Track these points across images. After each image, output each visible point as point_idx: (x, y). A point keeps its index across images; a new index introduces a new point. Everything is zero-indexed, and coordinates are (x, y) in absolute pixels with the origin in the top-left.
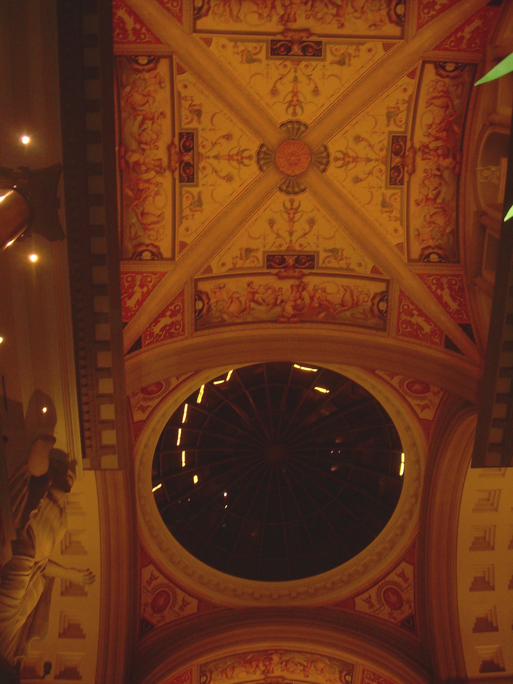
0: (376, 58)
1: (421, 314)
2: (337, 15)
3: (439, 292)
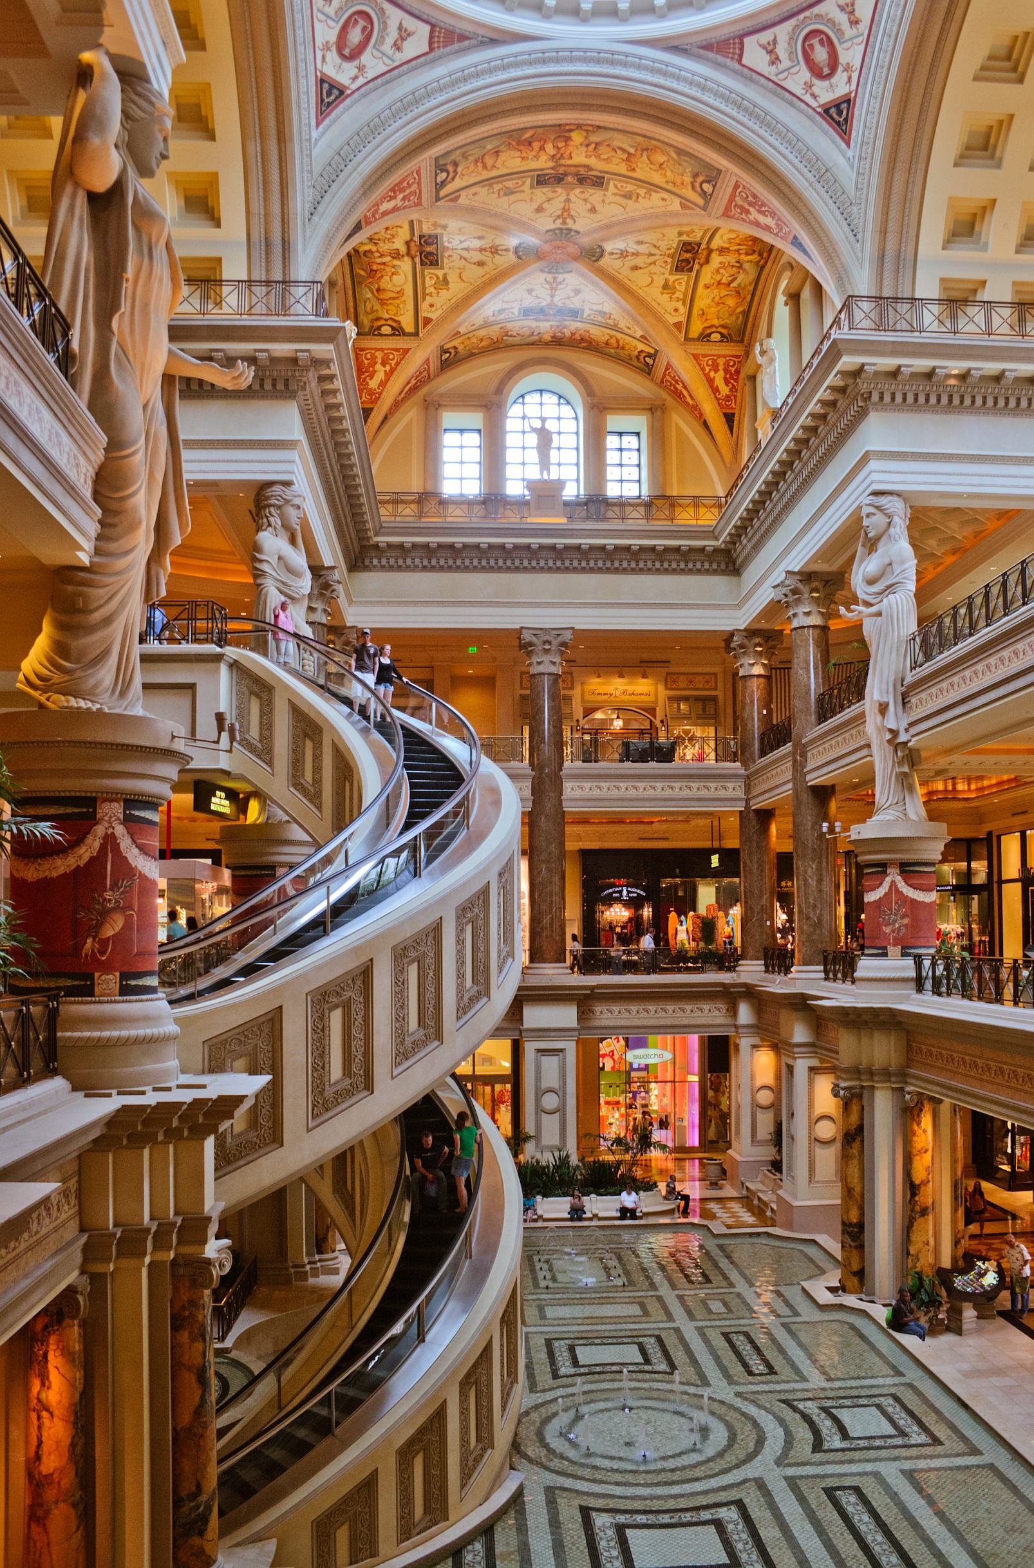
0: (667, 317)
1: (389, 375)
2: (719, 283)
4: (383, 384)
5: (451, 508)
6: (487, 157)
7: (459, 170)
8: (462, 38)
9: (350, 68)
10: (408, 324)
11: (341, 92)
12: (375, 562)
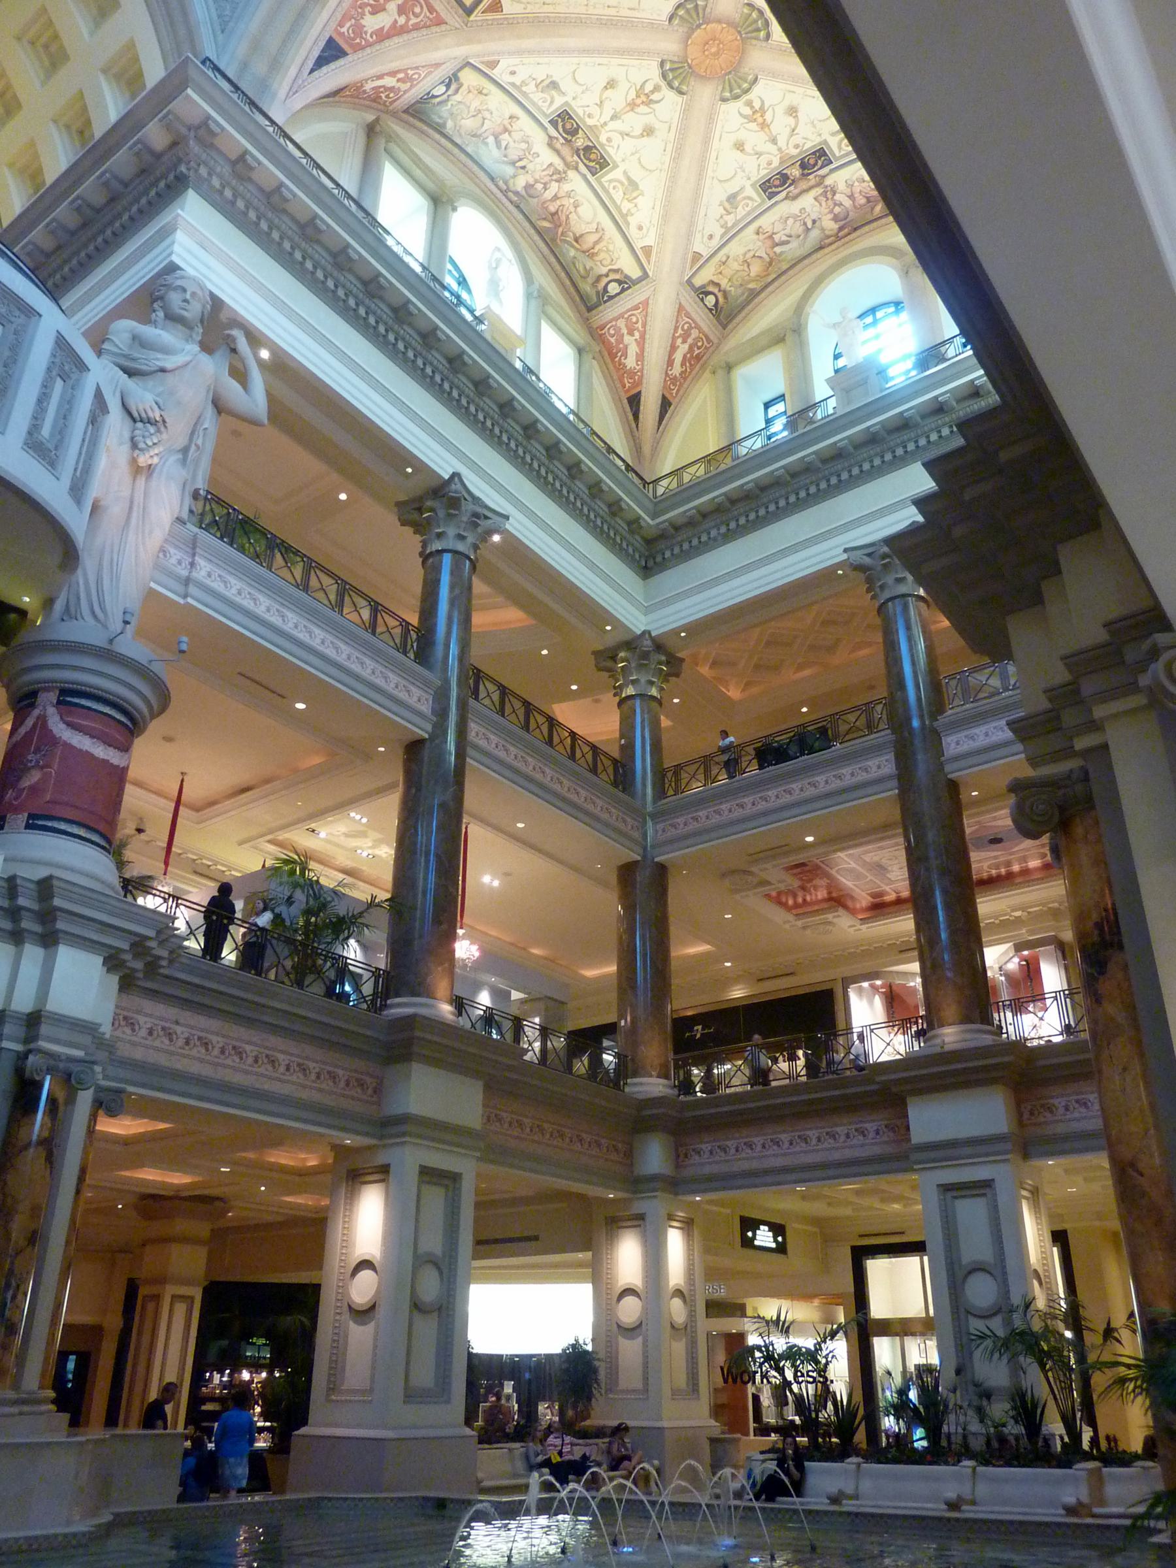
3: (680, 340)
4: (640, 357)
12: (668, 554)
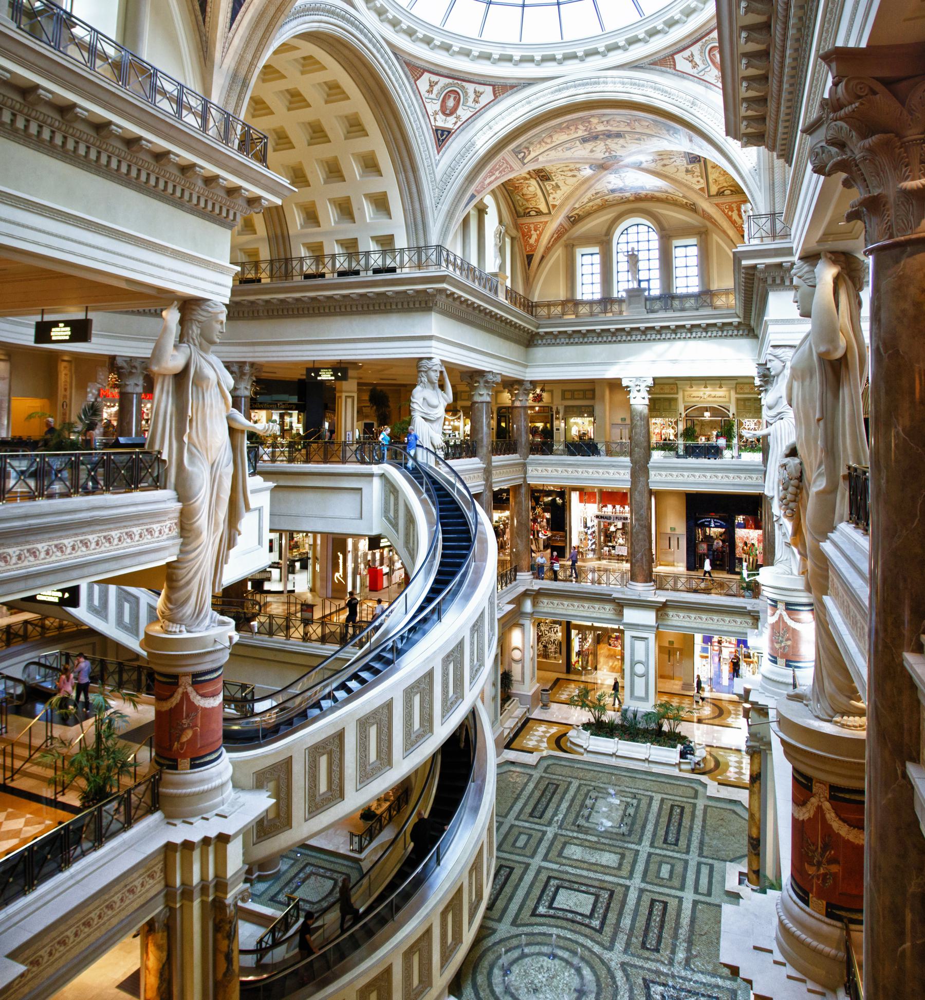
4: (537, 241)
5: (580, 308)
6: (545, 140)
7: (531, 149)
8: (512, 87)
9: (452, 119)
10: (543, 208)
11: (449, 132)
